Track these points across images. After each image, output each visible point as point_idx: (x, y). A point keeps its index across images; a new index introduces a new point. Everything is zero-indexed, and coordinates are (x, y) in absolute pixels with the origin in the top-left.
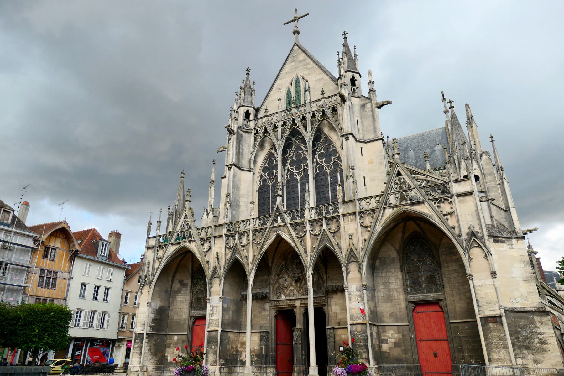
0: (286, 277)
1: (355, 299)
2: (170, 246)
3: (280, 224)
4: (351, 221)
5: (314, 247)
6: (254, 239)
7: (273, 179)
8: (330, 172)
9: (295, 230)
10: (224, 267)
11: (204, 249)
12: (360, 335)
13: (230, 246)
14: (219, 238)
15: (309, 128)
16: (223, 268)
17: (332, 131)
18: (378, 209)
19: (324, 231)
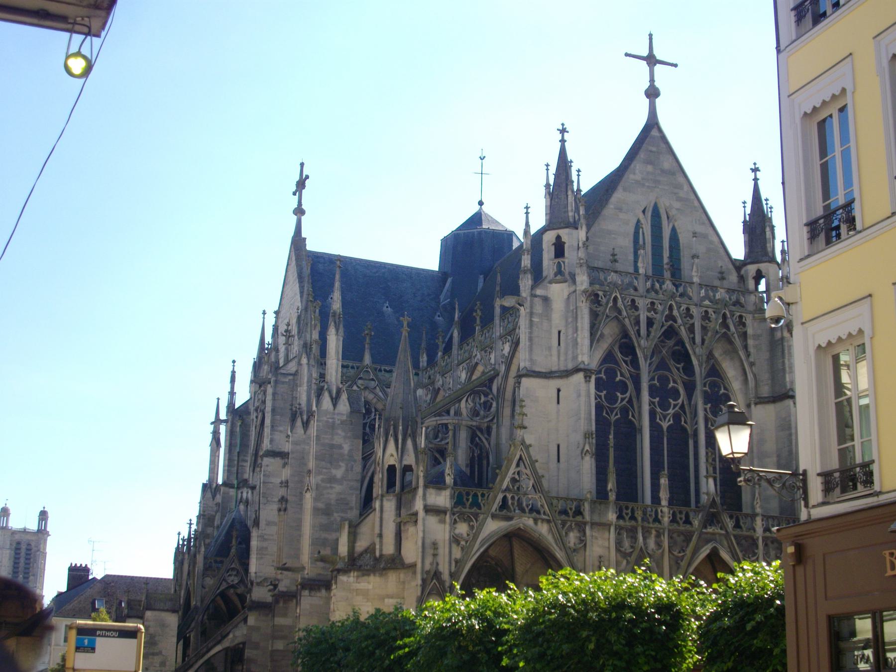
2: (489, 519)
15: (698, 339)
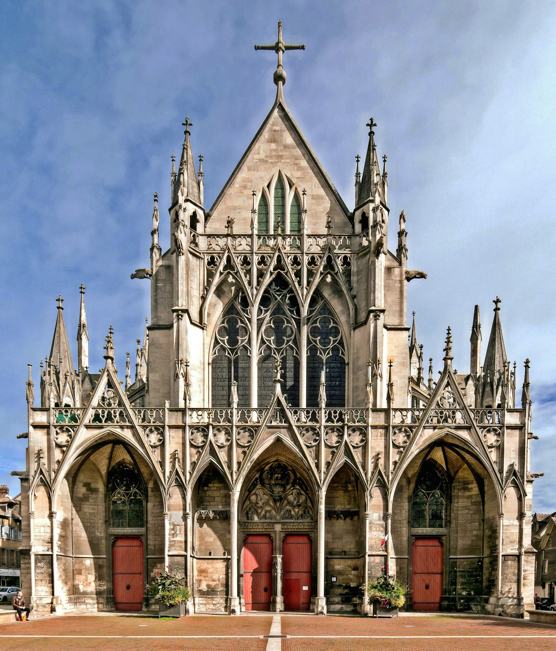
12: (378, 566)
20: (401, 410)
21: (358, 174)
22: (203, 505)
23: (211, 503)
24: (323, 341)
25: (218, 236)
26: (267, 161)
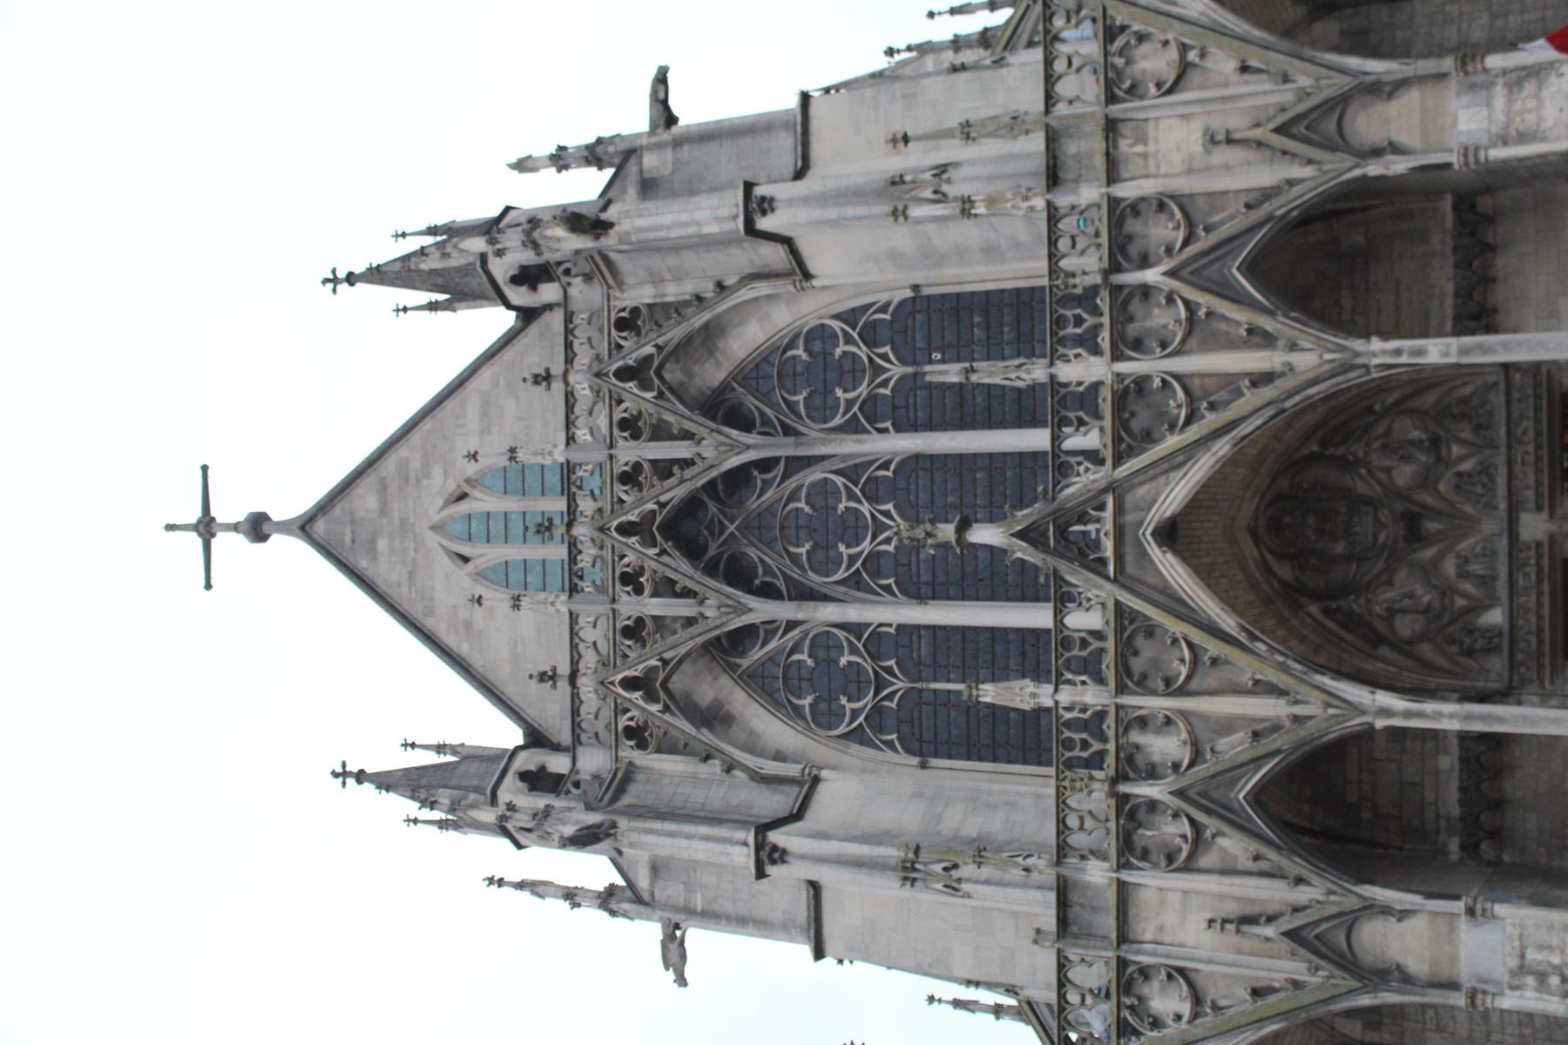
0: (1389, 595)
1: (1529, 111)
3: (1109, 526)
4: (1145, 143)
5: (1250, 331)
6: (1168, 682)
7: (882, 668)
8: (903, 361)
9: (1149, 438)
10: (1299, 881)
11: (1178, 1017)
13: (1184, 837)
14: (1132, 911)
15: (681, 450)
16: (1302, 888)
17: (721, 344)
18: (1110, 12)
19: (1172, 274)
20: (1050, 79)
21: (433, 307)
22: (1438, 831)
23: (1430, 796)
24: (848, 377)
25: (575, 712)
26: (414, 561)
